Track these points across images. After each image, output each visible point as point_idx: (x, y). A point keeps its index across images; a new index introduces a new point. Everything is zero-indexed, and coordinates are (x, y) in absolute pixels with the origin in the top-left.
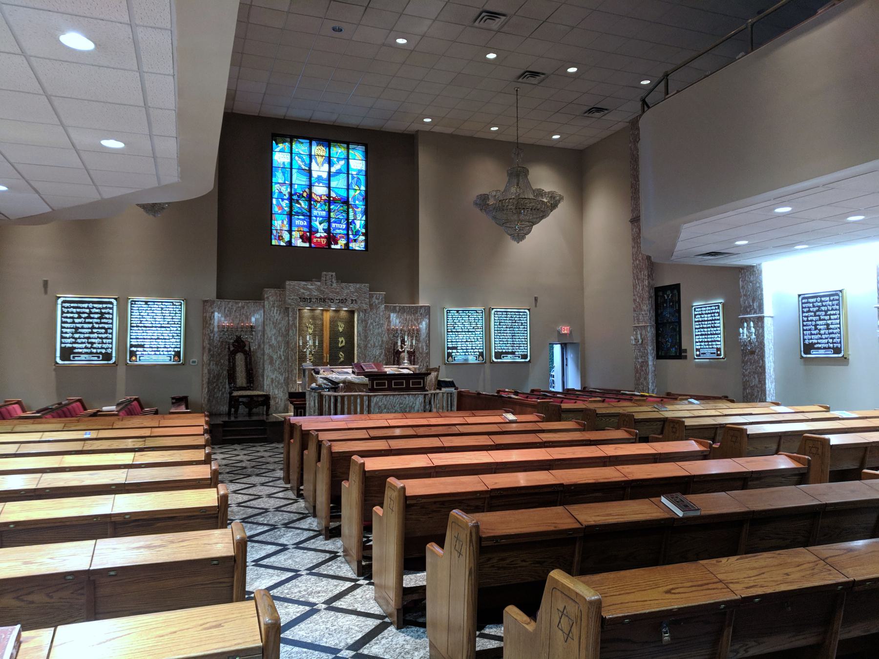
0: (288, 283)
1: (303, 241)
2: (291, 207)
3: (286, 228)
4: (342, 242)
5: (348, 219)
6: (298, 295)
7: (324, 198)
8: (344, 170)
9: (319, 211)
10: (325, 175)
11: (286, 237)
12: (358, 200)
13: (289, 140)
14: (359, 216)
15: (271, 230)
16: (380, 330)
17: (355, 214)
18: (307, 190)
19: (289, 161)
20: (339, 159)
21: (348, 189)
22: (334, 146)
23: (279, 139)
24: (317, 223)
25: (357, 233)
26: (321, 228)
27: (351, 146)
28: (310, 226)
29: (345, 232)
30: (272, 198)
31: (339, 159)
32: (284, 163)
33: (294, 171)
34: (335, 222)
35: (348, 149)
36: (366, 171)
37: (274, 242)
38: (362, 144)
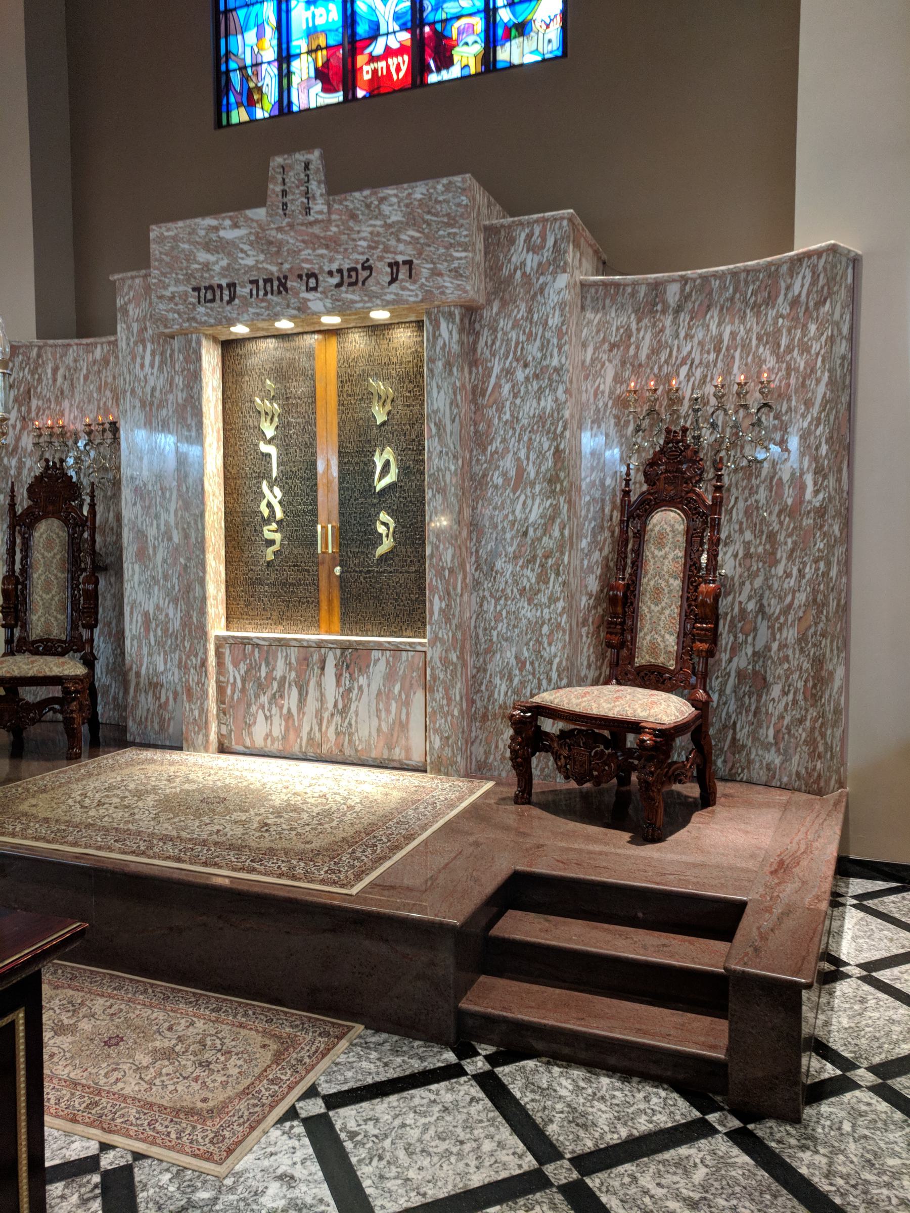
0: (155, 232)
6: (189, 277)
16: (548, 403)
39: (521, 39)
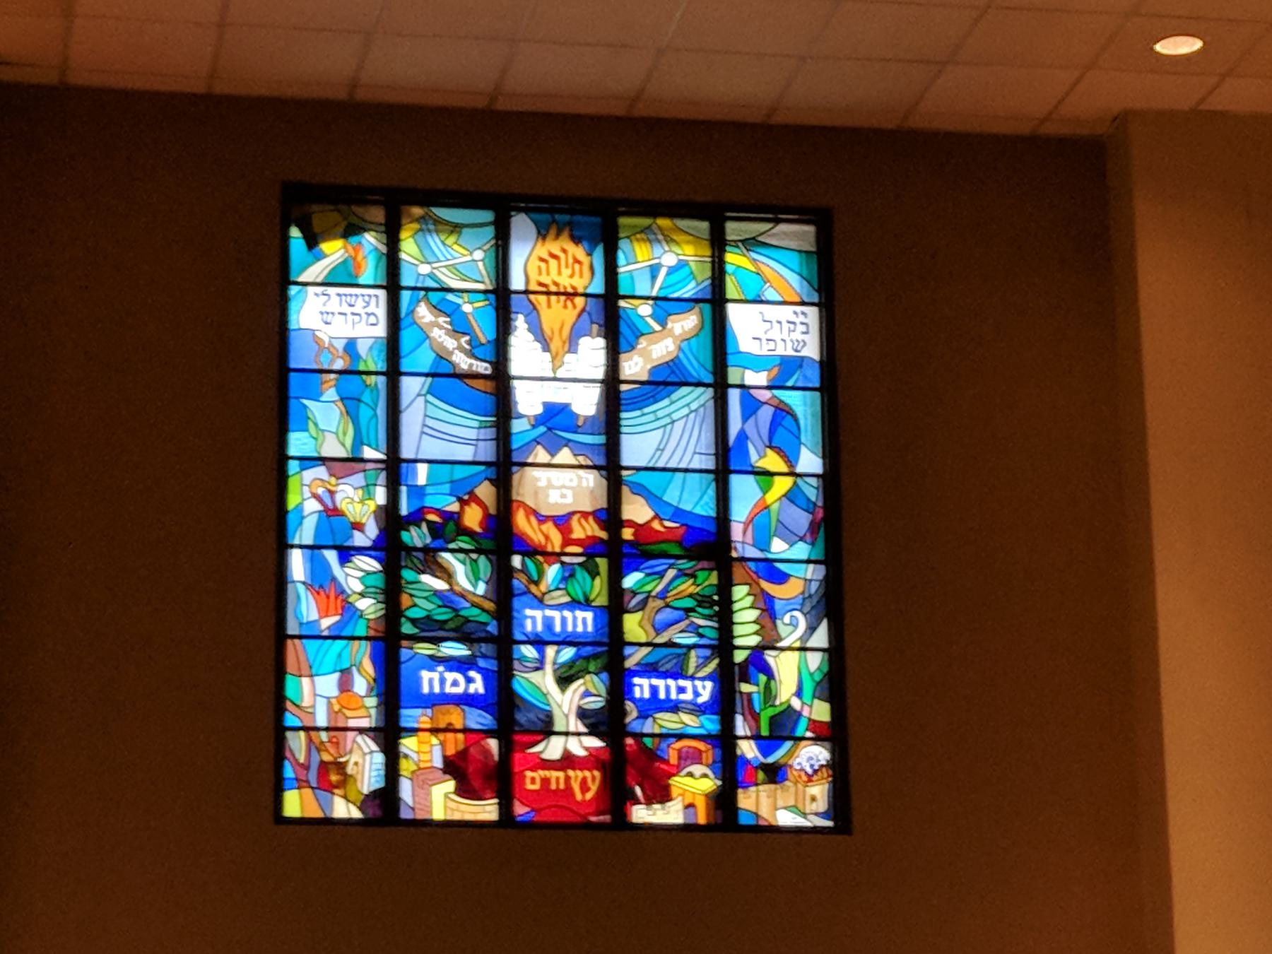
1: (466, 790)
2: (392, 591)
3: (367, 713)
4: (695, 785)
5: (724, 644)
7: (585, 529)
8: (699, 364)
9: (556, 610)
10: (586, 402)
11: (367, 765)
12: (791, 537)
13: (378, 214)
14: (793, 626)
15: (280, 731)
17: (768, 608)
18: (486, 491)
19: (381, 331)
20: (665, 304)
21: (721, 474)
22: (648, 235)
23: (321, 216)
24: (547, 680)
25: (781, 729)
26: (565, 703)
27: (734, 230)
28: (503, 702)
29: (710, 724)
30: (283, 546)
31: (665, 304)
32: (351, 346)
33: (411, 387)
34: (649, 669)
35: (718, 244)
36: (829, 364)
37: (294, 804)
38: (802, 214)
39: (772, 786)
